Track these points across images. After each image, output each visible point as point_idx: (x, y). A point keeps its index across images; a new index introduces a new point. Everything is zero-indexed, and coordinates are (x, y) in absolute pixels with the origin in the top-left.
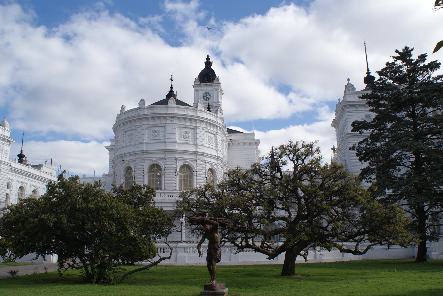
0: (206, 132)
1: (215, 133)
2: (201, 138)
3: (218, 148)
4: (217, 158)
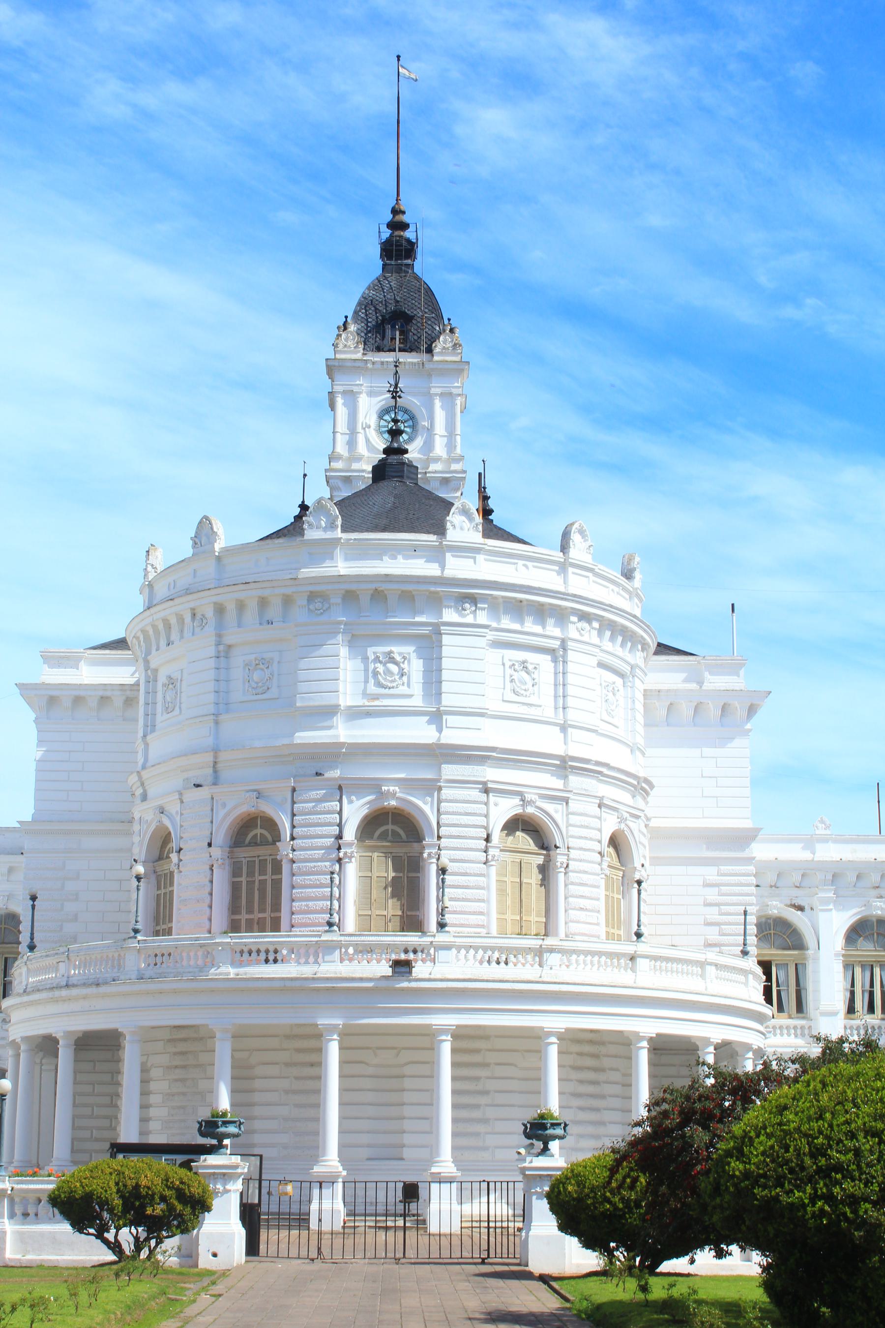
1: (556, 644)
3: (573, 716)
4: (565, 766)
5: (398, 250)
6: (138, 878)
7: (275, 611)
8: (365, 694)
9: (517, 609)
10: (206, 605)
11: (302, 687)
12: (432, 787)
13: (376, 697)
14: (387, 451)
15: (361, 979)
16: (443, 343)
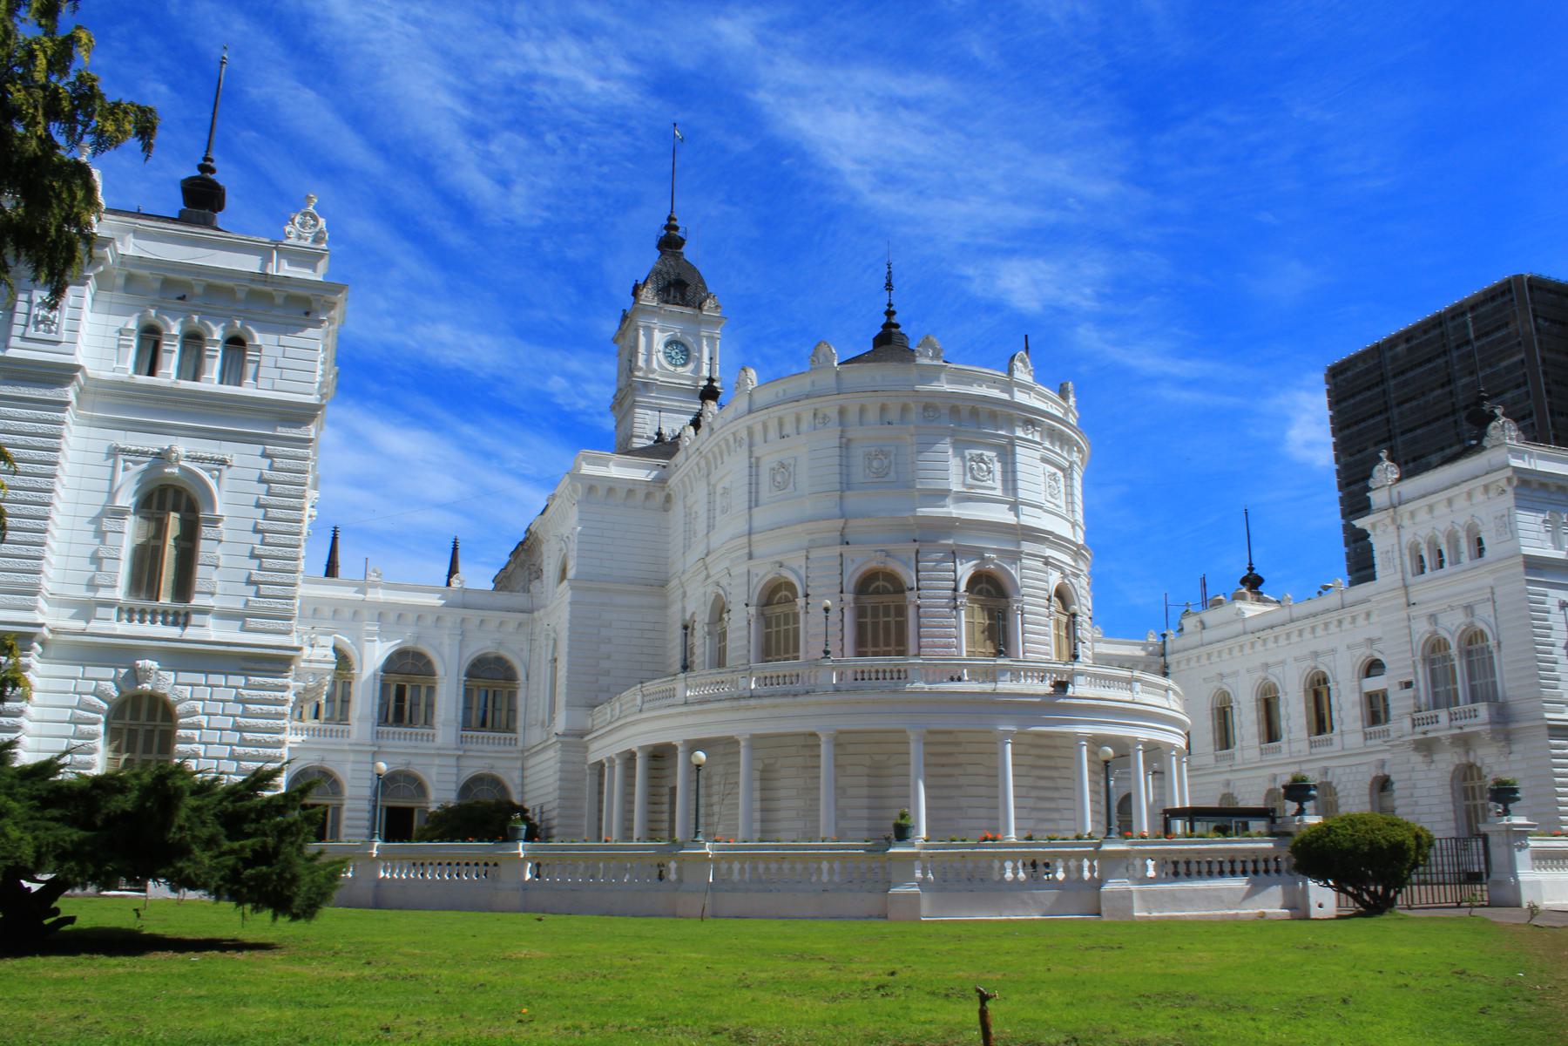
0: (1045, 460)
1: (1066, 464)
2: (1030, 478)
5: (670, 242)
6: (827, 610)
7: (893, 414)
8: (964, 484)
9: (1054, 435)
10: (830, 407)
11: (922, 474)
12: (1016, 557)
13: (972, 487)
14: (884, 326)
15: (1032, 696)
16: (709, 303)
